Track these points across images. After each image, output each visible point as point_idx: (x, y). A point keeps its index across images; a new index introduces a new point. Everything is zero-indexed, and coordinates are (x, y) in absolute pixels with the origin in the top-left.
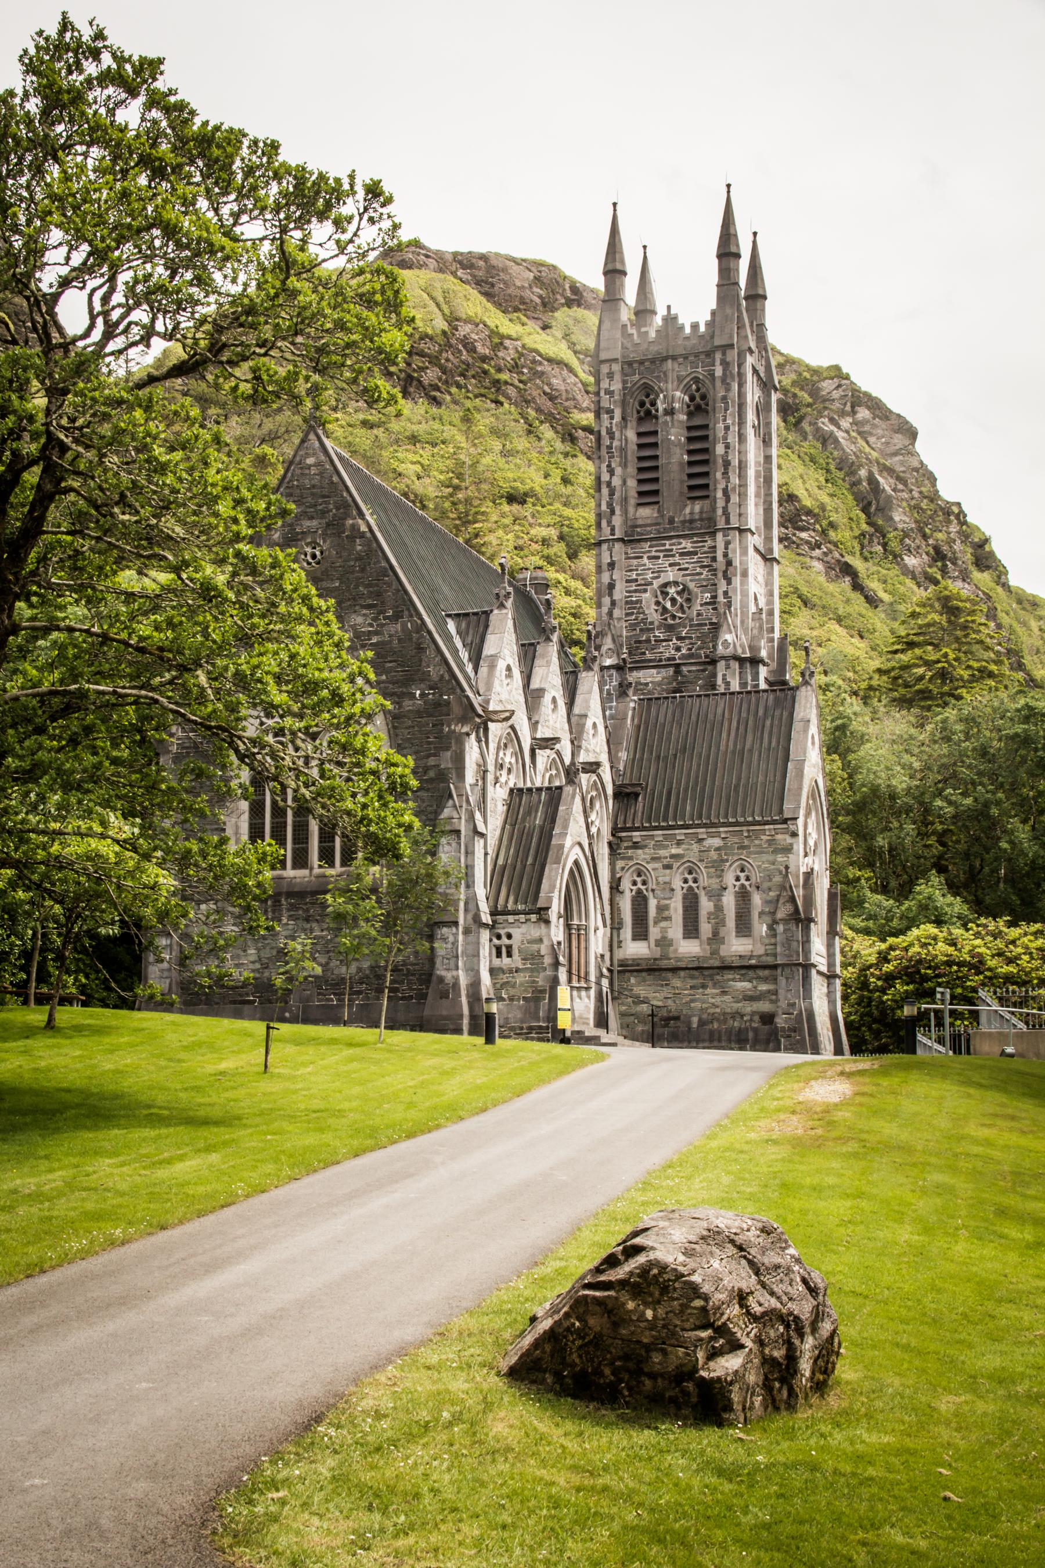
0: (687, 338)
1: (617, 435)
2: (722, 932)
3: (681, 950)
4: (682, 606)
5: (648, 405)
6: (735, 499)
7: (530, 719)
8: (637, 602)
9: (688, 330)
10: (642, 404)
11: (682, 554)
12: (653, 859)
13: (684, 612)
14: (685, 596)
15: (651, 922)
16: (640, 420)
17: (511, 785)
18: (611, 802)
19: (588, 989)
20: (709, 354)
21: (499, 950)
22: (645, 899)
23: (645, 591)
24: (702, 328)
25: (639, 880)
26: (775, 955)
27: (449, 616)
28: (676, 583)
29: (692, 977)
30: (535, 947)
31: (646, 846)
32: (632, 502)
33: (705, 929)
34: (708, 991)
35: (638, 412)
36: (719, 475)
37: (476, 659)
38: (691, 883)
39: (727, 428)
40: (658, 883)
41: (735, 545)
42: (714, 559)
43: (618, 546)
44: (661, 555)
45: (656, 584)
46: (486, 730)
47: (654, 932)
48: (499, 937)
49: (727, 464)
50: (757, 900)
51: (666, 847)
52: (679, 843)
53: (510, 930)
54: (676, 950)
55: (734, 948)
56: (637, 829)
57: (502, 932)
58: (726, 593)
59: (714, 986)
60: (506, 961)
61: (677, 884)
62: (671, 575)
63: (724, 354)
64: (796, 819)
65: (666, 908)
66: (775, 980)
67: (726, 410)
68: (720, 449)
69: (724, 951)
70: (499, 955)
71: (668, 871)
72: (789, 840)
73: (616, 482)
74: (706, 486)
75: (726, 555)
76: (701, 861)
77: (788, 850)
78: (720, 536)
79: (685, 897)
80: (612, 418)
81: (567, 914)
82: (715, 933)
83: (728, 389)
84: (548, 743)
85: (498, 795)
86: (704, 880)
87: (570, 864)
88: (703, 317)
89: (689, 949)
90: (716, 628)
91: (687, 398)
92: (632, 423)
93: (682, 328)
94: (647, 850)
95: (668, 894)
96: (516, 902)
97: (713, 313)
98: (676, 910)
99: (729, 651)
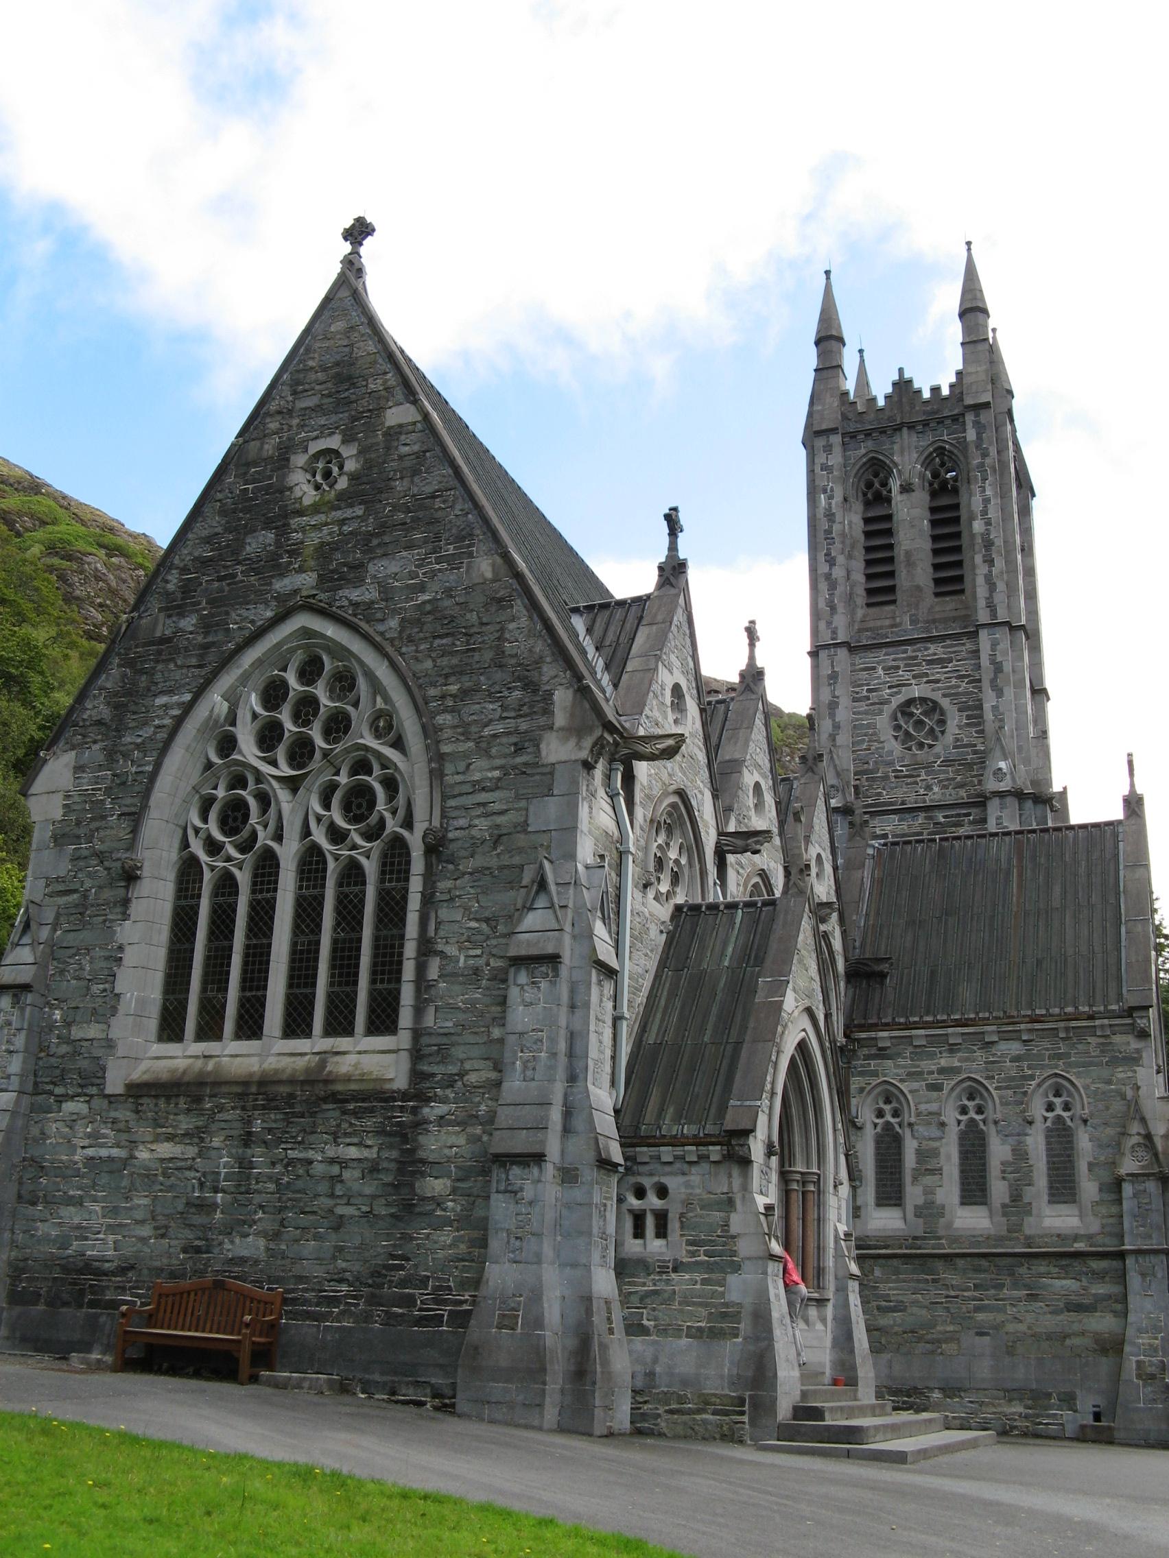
0: (927, 402)
1: (838, 518)
2: (1028, 1194)
3: (958, 1223)
4: (932, 730)
5: (877, 485)
6: (1001, 586)
7: (715, 797)
8: (869, 726)
9: (926, 394)
10: (869, 485)
11: (930, 662)
12: (912, 1076)
13: (936, 739)
14: (936, 717)
15: (908, 1178)
16: (868, 504)
17: (680, 899)
18: (842, 984)
19: (821, 1302)
20: (957, 419)
21: (638, 1219)
22: (897, 1140)
23: (880, 712)
24: (945, 391)
25: (887, 1108)
26: (1121, 1237)
27: (576, 610)
28: (923, 700)
29: (978, 1270)
30: (717, 1216)
31: (899, 1055)
32: (861, 598)
33: (999, 1190)
34: (1005, 1292)
35: (865, 494)
36: (978, 559)
37: (616, 666)
38: (972, 1114)
39: (986, 501)
40: (918, 1114)
41: (1005, 644)
42: (978, 667)
43: (842, 653)
44: (901, 664)
45: (896, 701)
46: (629, 779)
47: (913, 1194)
48: (640, 1193)
49: (988, 544)
50: (1084, 1142)
51: (932, 1056)
52: (953, 1048)
53: (664, 1180)
54: (949, 1225)
55: (1047, 1222)
56: (887, 1026)
57: (647, 1182)
58: (995, 708)
59: (1015, 1286)
60: (655, 1246)
61: (951, 1115)
62: (916, 692)
63: (977, 415)
64: (1147, 1008)
65: (935, 1153)
66: (1122, 1278)
67: (984, 479)
68: (978, 526)
69: (1030, 1226)
70: (639, 1233)
71: (935, 1094)
72: (1135, 1044)
73: (838, 573)
74: (960, 579)
75: (993, 662)
76: (988, 1078)
77: (1133, 1060)
78: (983, 635)
79: (963, 1137)
80: (831, 497)
81: (782, 1149)
82: (1016, 1197)
83: (985, 455)
84: (749, 841)
85: (649, 911)
86: (995, 1110)
87: (789, 1048)
88: (945, 382)
89: (972, 1221)
90: (982, 759)
91: (928, 474)
92: (858, 507)
93: (919, 392)
94: (901, 1061)
95: (935, 1133)
96: (677, 1119)
97: (959, 374)
98: (949, 1157)
99: (1004, 786)
